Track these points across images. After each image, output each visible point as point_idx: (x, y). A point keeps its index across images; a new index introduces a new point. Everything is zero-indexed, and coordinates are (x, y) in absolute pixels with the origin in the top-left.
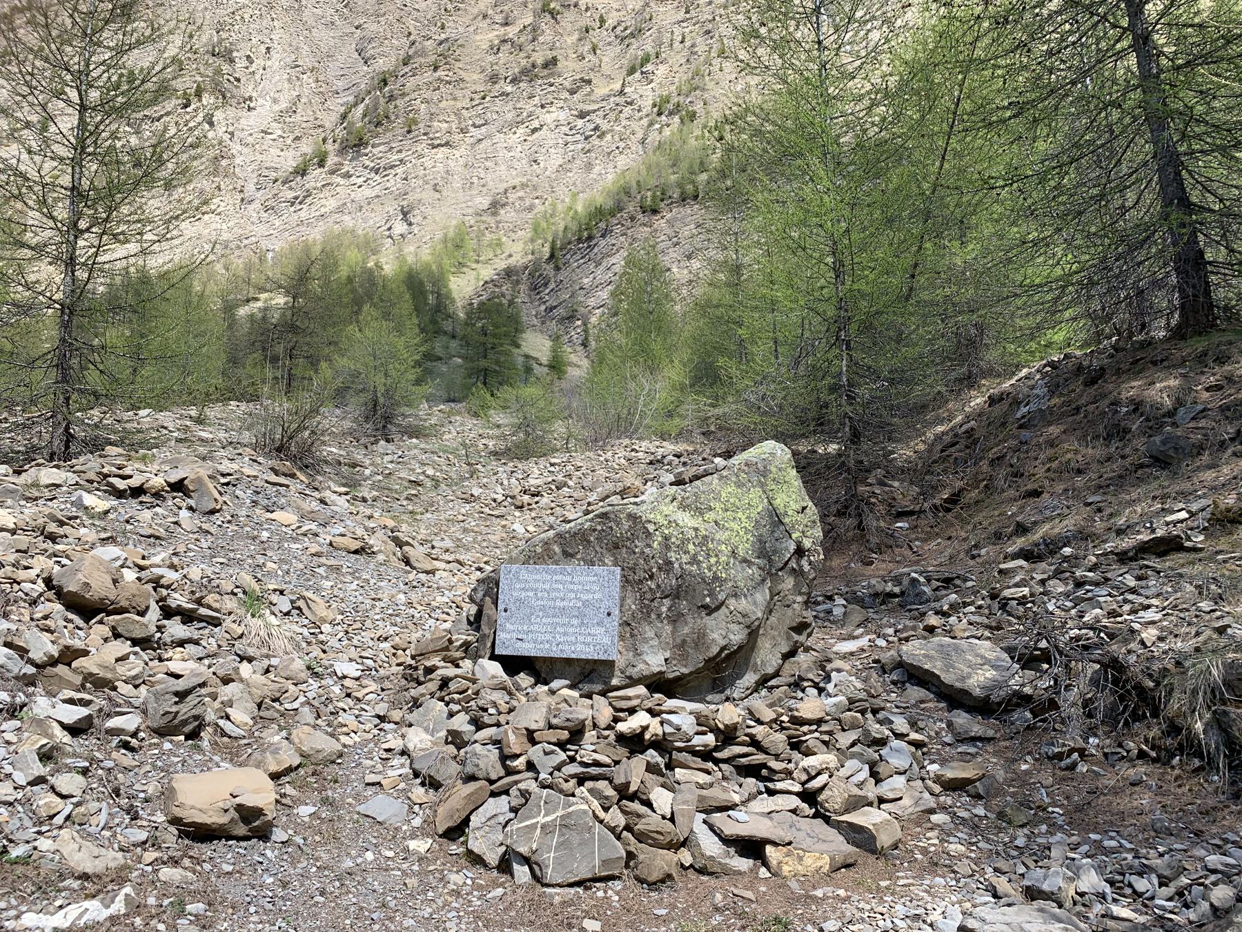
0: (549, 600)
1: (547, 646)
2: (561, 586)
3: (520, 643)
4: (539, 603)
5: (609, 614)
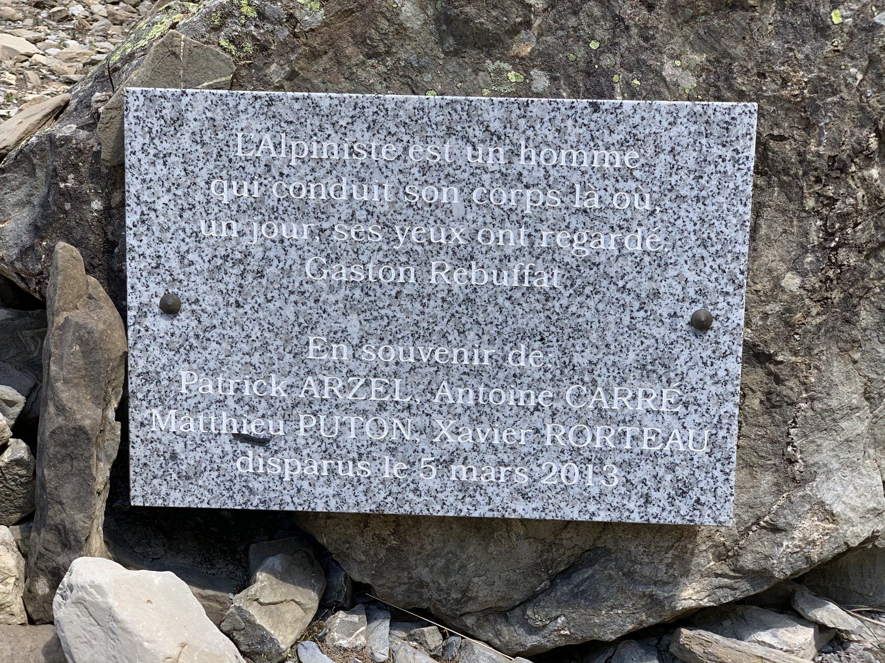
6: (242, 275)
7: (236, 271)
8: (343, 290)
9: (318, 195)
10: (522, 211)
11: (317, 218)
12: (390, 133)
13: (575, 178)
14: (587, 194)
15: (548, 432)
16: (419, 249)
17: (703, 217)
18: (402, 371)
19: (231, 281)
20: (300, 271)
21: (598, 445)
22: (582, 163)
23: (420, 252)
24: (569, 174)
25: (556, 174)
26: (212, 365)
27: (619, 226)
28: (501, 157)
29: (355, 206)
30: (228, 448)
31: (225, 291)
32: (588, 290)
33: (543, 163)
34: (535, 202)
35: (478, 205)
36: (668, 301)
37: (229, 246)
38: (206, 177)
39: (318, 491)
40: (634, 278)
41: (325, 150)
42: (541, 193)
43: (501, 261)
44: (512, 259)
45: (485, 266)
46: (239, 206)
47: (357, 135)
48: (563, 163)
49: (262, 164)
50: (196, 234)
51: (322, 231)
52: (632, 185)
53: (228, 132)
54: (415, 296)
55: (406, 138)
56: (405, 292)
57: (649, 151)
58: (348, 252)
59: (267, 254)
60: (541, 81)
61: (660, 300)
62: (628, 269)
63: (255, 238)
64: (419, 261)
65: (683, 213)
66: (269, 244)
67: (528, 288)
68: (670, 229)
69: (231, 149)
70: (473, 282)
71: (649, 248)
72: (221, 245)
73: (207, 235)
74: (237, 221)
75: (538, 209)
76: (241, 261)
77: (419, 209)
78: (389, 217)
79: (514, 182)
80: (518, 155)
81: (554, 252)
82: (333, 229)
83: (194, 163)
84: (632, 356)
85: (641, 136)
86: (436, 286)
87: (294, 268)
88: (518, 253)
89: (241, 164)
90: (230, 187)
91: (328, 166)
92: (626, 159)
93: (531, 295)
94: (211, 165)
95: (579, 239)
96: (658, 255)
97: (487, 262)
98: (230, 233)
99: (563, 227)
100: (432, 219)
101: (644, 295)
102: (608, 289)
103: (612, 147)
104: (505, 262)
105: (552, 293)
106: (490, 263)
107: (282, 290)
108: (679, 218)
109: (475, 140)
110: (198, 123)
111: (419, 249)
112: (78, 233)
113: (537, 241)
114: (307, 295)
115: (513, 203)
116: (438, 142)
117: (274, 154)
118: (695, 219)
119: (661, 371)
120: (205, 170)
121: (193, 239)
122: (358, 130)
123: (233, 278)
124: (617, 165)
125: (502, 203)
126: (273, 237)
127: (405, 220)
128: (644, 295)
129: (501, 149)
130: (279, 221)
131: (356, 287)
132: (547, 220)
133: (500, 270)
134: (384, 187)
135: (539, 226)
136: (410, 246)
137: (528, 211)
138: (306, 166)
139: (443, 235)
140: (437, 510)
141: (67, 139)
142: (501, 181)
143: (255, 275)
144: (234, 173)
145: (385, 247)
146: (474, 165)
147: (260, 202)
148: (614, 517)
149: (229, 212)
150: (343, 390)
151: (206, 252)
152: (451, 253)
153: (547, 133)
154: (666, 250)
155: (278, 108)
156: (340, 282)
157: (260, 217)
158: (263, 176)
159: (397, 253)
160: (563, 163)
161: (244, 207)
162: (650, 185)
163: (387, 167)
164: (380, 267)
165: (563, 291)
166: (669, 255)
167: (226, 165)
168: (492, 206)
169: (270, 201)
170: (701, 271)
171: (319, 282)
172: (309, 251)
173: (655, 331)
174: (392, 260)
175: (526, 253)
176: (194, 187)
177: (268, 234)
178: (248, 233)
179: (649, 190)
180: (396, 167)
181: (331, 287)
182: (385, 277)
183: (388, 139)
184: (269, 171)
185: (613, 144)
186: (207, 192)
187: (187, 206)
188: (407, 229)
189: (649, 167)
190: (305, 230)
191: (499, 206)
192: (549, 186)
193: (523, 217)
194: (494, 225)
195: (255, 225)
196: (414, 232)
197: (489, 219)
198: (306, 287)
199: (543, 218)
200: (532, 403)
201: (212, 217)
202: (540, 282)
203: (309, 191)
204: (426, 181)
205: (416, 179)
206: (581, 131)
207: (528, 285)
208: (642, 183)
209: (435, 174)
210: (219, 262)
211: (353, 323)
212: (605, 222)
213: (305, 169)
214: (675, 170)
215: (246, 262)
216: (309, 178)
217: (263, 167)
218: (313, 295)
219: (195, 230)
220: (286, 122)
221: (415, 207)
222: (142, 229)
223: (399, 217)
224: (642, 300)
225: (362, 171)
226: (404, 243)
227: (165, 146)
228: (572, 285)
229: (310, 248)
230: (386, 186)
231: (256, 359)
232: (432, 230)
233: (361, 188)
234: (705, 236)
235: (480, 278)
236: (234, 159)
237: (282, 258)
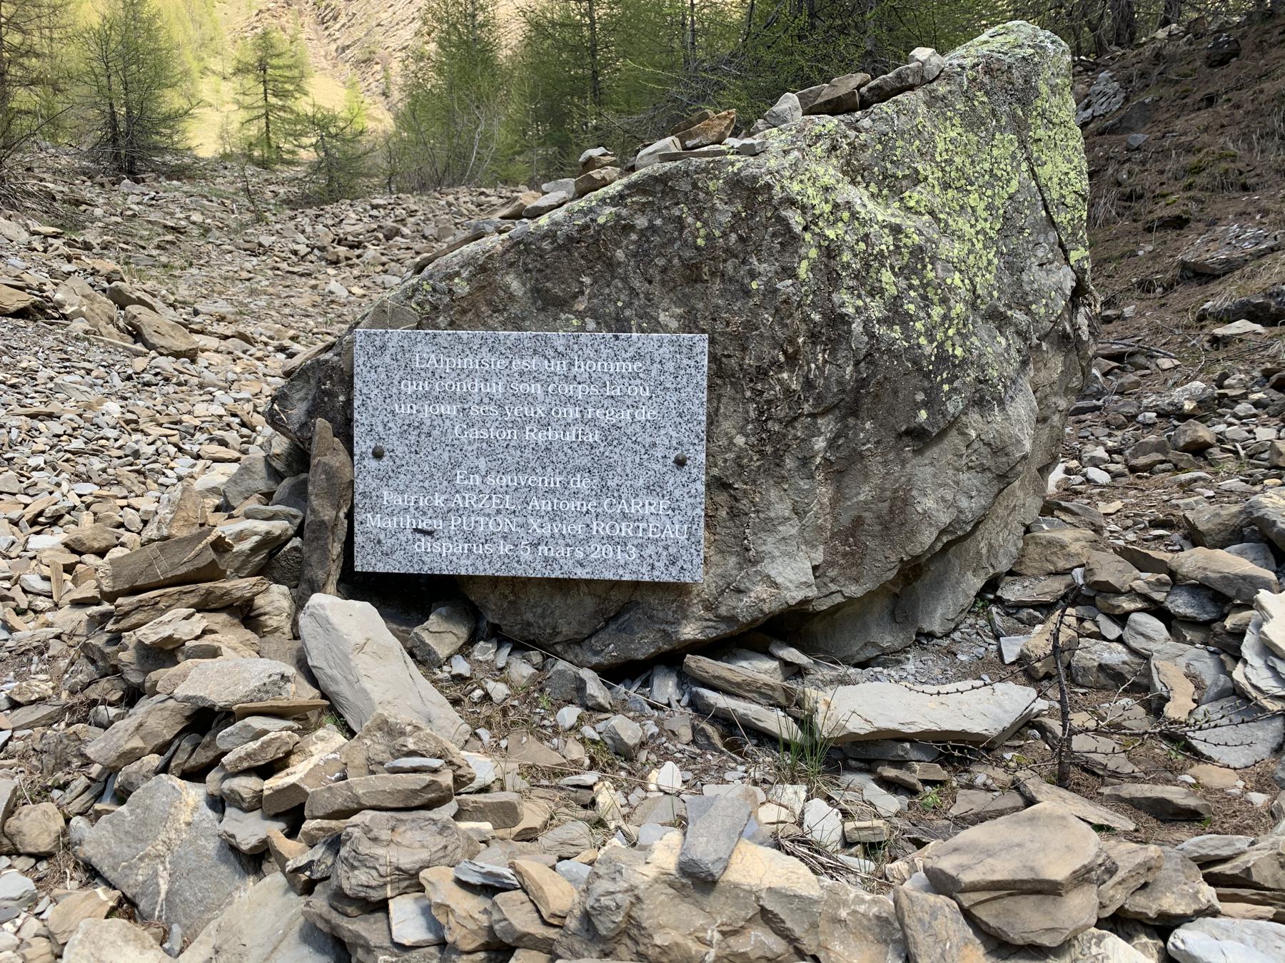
0: (503, 425)
1: (504, 548)
2: (536, 389)
3: (425, 541)
4: (475, 433)
5: (680, 463)
7: (416, 433)
13: (606, 378)
15: (595, 528)
18: (510, 490)
21: (623, 534)
26: (401, 487)
30: (410, 537)
32: (615, 443)
39: (462, 562)
50: (393, 412)
52: (638, 381)
84: (641, 481)
94: (401, 372)
119: (658, 490)
140: (531, 574)
148: (634, 577)
150: (477, 502)
155: (439, 340)
173: (654, 466)
180: (505, 372)
189: (648, 371)
200: (584, 509)
211: (482, 463)
213: (453, 374)
222: (363, 409)
227: (376, 362)
231: (426, 484)
235: (554, 436)
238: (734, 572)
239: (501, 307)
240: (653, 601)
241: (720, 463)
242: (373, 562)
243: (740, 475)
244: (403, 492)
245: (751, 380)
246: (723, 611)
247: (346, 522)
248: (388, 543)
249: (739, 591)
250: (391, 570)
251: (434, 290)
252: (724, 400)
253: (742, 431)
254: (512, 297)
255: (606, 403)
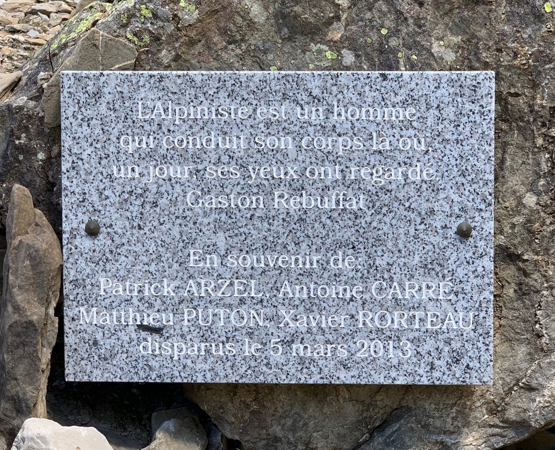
6: (142, 205)
7: (138, 202)
8: (213, 215)
9: (194, 145)
10: (337, 153)
11: (194, 162)
12: (243, 99)
13: (372, 128)
14: (381, 140)
15: (360, 317)
16: (266, 183)
17: (461, 154)
18: (256, 273)
19: (135, 210)
20: (183, 201)
21: (396, 326)
22: (377, 117)
23: (267, 185)
24: (368, 125)
25: (359, 125)
26: (122, 273)
27: (404, 162)
28: (321, 115)
29: (220, 153)
30: (134, 335)
31: (130, 218)
33: (350, 117)
34: (345, 146)
35: (306, 150)
36: (440, 217)
37: (133, 184)
38: (117, 134)
39: (198, 366)
40: (416, 200)
41: (199, 112)
42: (349, 139)
43: (323, 190)
44: (331, 188)
45: (312, 194)
46: (140, 155)
47: (221, 101)
48: (364, 118)
49: (156, 123)
50: (110, 176)
51: (198, 171)
52: (412, 132)
53: (132, 101)
54: (264, 218)
55: (255, 102)
56: (257, 215)
57: (422, 108)
58: (216, 186)
59: (160, 189)
60: (349, 58)
61: (435, 216)
62: (412, 194)
63: (151, 178)
64: (266, 192)
65: (448, 152)
66: (161, 182)
67: (342, 210)
68: (439, 164)
69: (134, 113)
70: (304, 206)
71: (426, 178)
72: (128, 183)
73: (118, 176)
74: (138, 166)
75: (347, 152)
76: (141, 195)
77: (265, 153)
78: (244, 160)
79: (330, 133)
80: (332, 113)
81: (360, 182)
82: (206, 170)
83: (109, 124)
84: (417, 258)
85: (416, 97)
86: (278, 210)
87: (178, 199)
88: (334, 184)
89: (141, 124)
90: (134, 141)
91: (201, 124)
92: (407, 113)
93: (344, 215)
94: (120, 126)
95: (377, 172)
96: (432, 183)
97: (313, 191)
98: (133, 174)
99: (365, 164)
100: (274, 160)
101: (423, 213)
102: (398, 209)
103: (397, 105)
104: (326, 190)
105: (359, 213)
106: (315, 192)
107: (171, 215)
108: (445, 155)
109: (302, 102)
110: (111, 96)
111: (266, 183)
112: (28, 177)
113: (348, 175)
114: (188, 219)
115: (330, 147)
116: (277, 105)
117: (164, 116)
118: (456, 156)
119: (438, 269)
120: (116, 129)
121: (108, 180)
122: (221, 97)
123: (136, 208)
124: (401, 118)
125: (323, 148)
126: (163, 177)
127: (255, 162)
128: (423, 213)
129: (320, 109)
130: (168, 164)
131: (222, 212)
132: (354, 159)
133: (322, 197)
134: (240, 138)
135: (348, 164)
136: (259, 180)
137: (340, 153)
138: (186, 124)
139: (282, 172)
140: (283, 380)
141: (21, 108)
142: (321, 132)
143: (151, 205)
144: (136, 131)
145: (242, 182)
146: (302, 121)
147: (155, 151)
148: (409, 380)
149: (133, 159)
150: (215, 289)
151: (117, 189)
152: (288, 185)
153: (352, 96)
154: (438, 179)
155: (166, 83)
156: (211, 208)
157: (155, 162)
158: (156, 133)
159: (250, 186)
160: (364, 118)
161: (143, 155)
162: (424, 132)
163: (242, 123)
164: (238, 197)
165: (367, 211)
166: (440, 182)
167: (131, 125)
168: (316, 150)
169: (161, 150)
170: (462, 194)
171: (196, 209)
172: (189, 186)
173: (432, 239)
174: (247, 192)
175: (340, 184)
176: (108, 142)
177: (160, 174)
178: (146, 174)
179: (424, 136)
180: (248, 123)
181: (205, 212)
182: (242, 204)
183: (242, 103)
184: (160, 128)
185: (398, 103)
186: (118, 145)
187: (104, 156)
188: (257, 168)
190: (186, 171)
191: (320, 150)
192: (355, 134)
193: (337, 157)
194: (317, 164)
195: (151, 168)
196: (262, 171)
197: (314, 160)
198: (188, 213)
199: (351, 158)
200: (348, 296)
201: (121, 163)
202: (351, 205)
203: (188, 142)
204: (269, 133)
205: (262, 132)
206: (375, 94)
207: (343, 208)
208: (419, 130)
209: (275, 127)
210: (127, 196)
211: (221, 240)
212: (394, 158)
213: (185, 127)
214: (440, 121)
215: (145, 196)
216: (188, 133)
217: (156, 126)
218: (193, 219)
219: (110, 173)
220: (172, 93)
221: (262, 152)
222: (73, 173)
223: (251, 160)
224: (422, 217)
225: (225, 126)
226: (255, 179)
227: (89, 113)
228: (373, 207)
229: (190, 184)
230: (242, 137)
231: (153, 268)
232: (275, 169)
233: (224, 139)
234: (464, 168)
235: (309, 203)
236: (136, 120)
237: (170, 192)
238: (524, 365)
239: (238, 37)
240: (429, 406)
241: (508, 229)
242: (89, 368)
243: (530, 243)
244: (123, 279)
245: (544, 125)
246: (511, 414)
247: (56, 320)
248: (106, 344)
249: (530, 389)
250: (111, 378)
251: (155, 16)
252: (511, 150)
253: (532, 188)
254: (251, 24)
255: (372, 159)
